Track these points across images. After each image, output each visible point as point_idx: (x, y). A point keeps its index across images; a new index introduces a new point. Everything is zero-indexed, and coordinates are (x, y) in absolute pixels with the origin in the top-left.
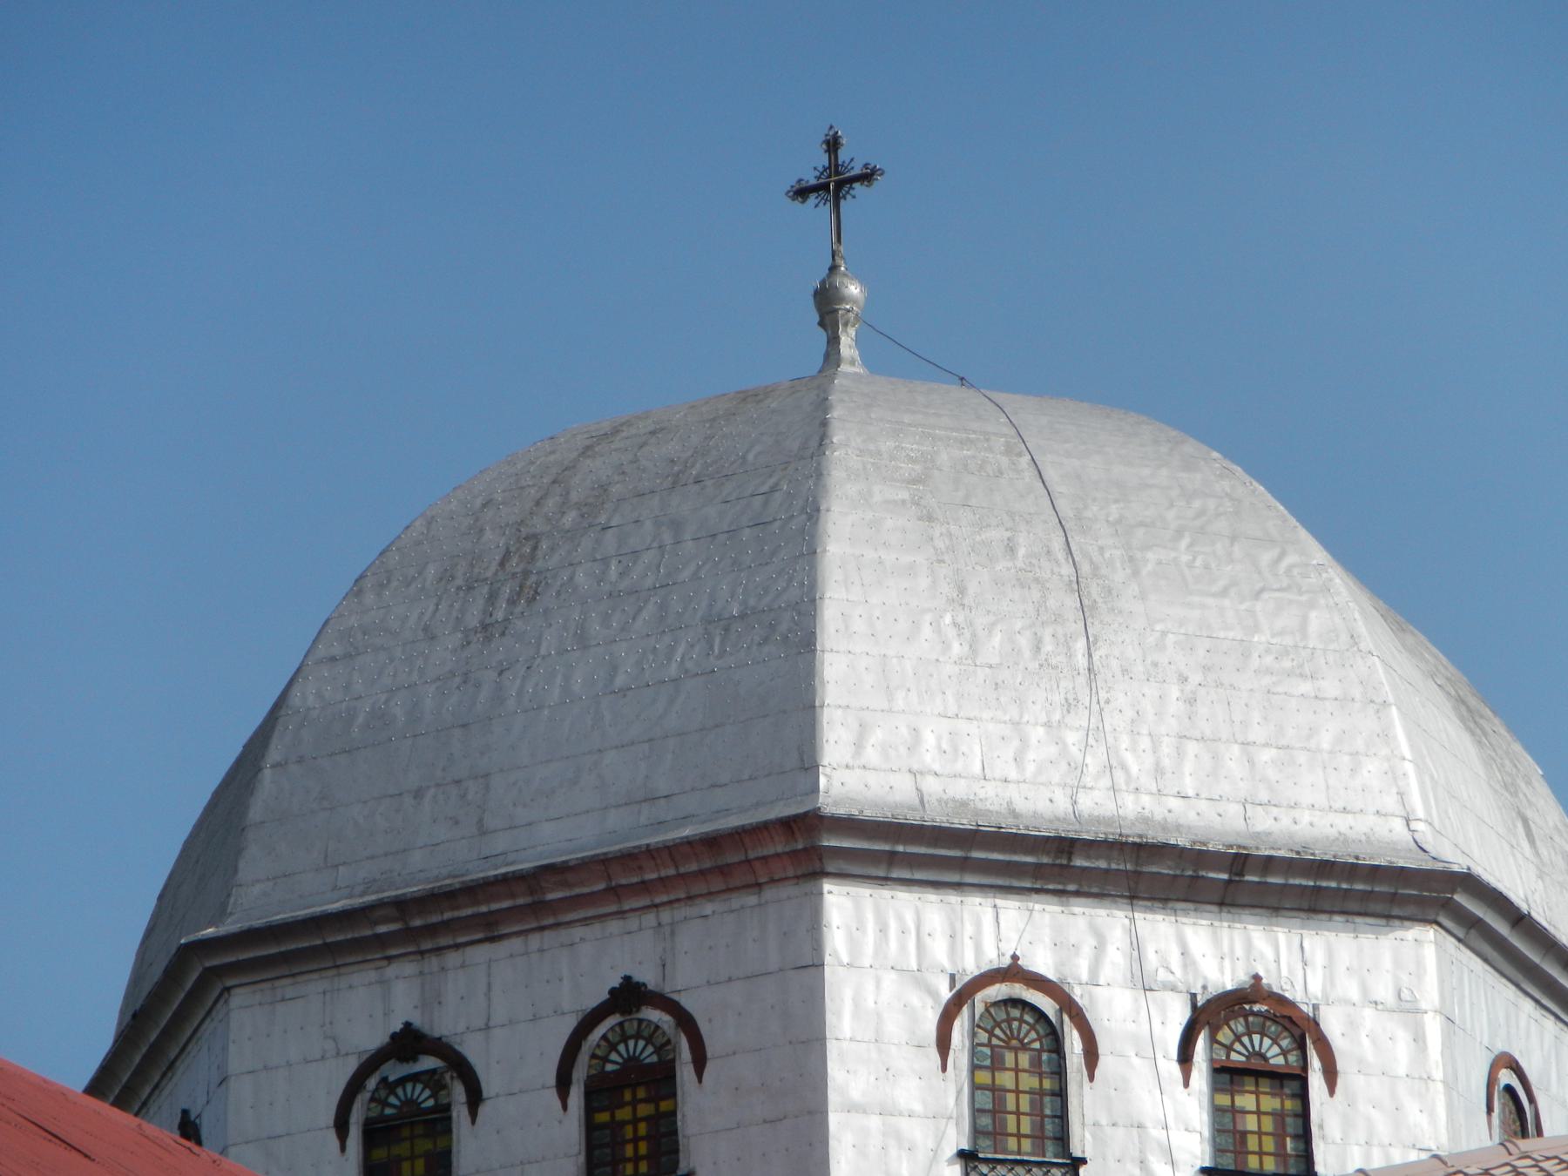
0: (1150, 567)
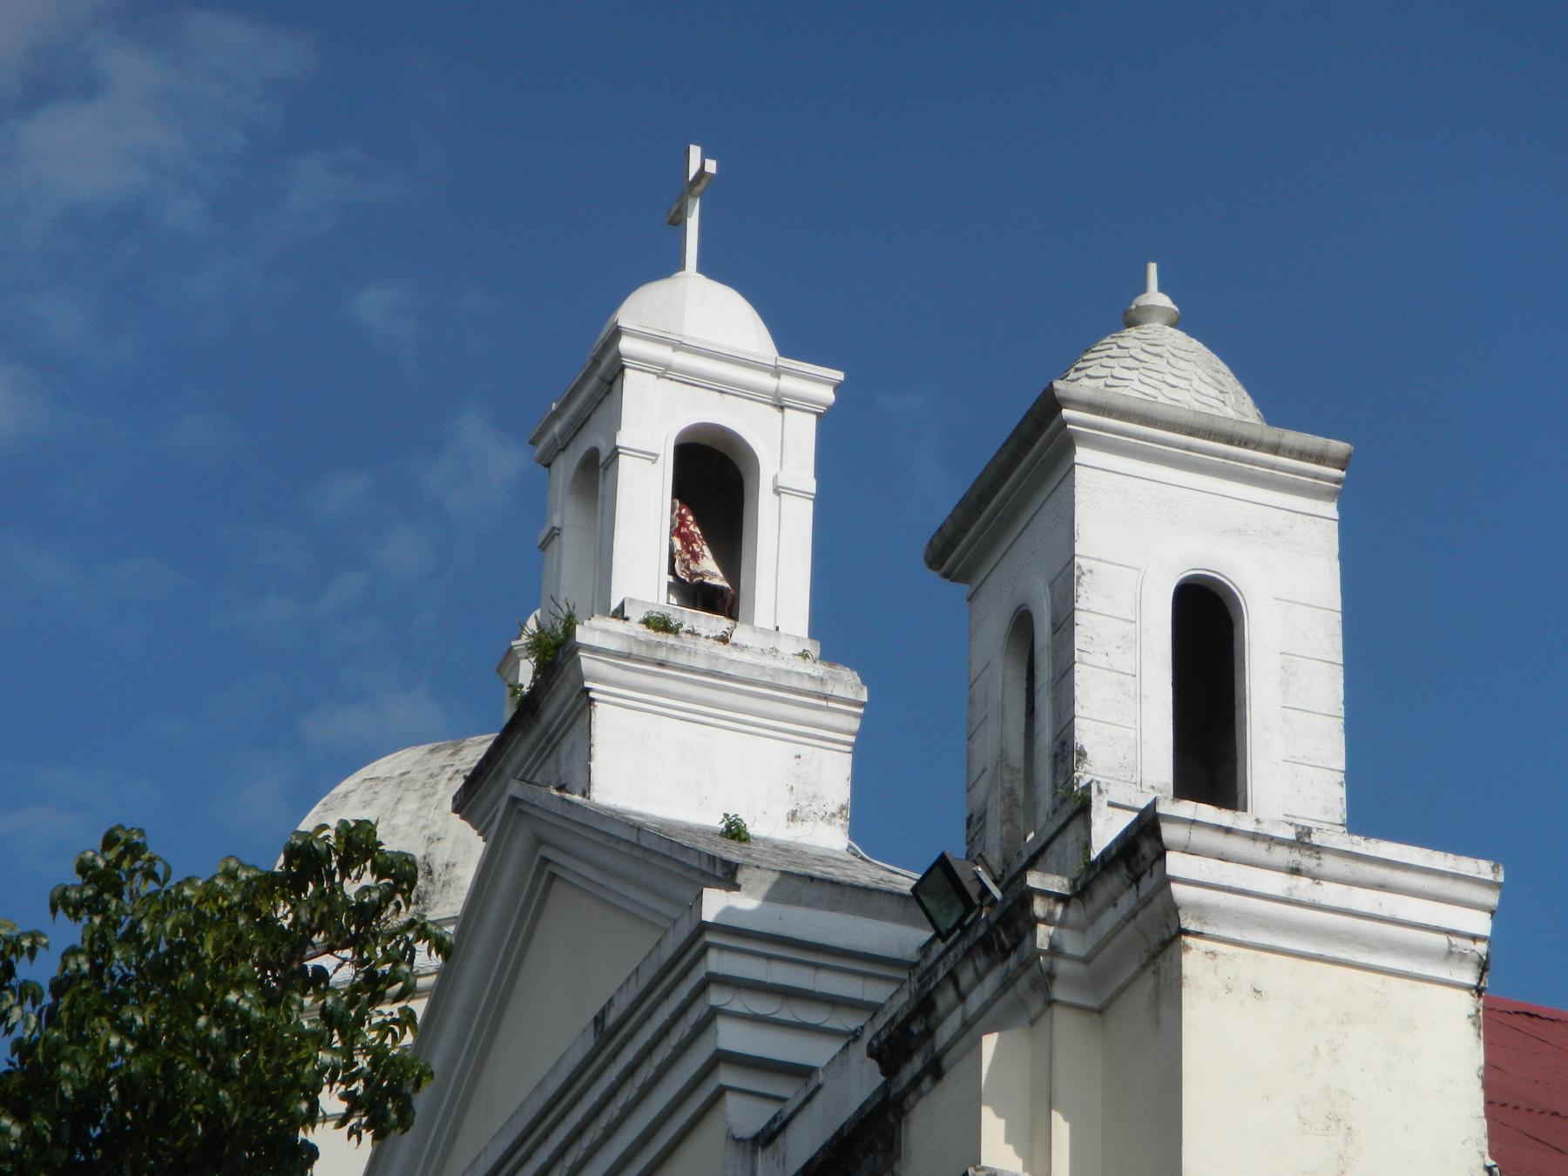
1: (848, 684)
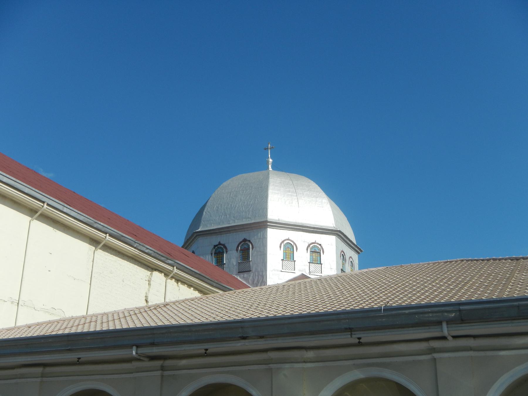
0: (305, 194)
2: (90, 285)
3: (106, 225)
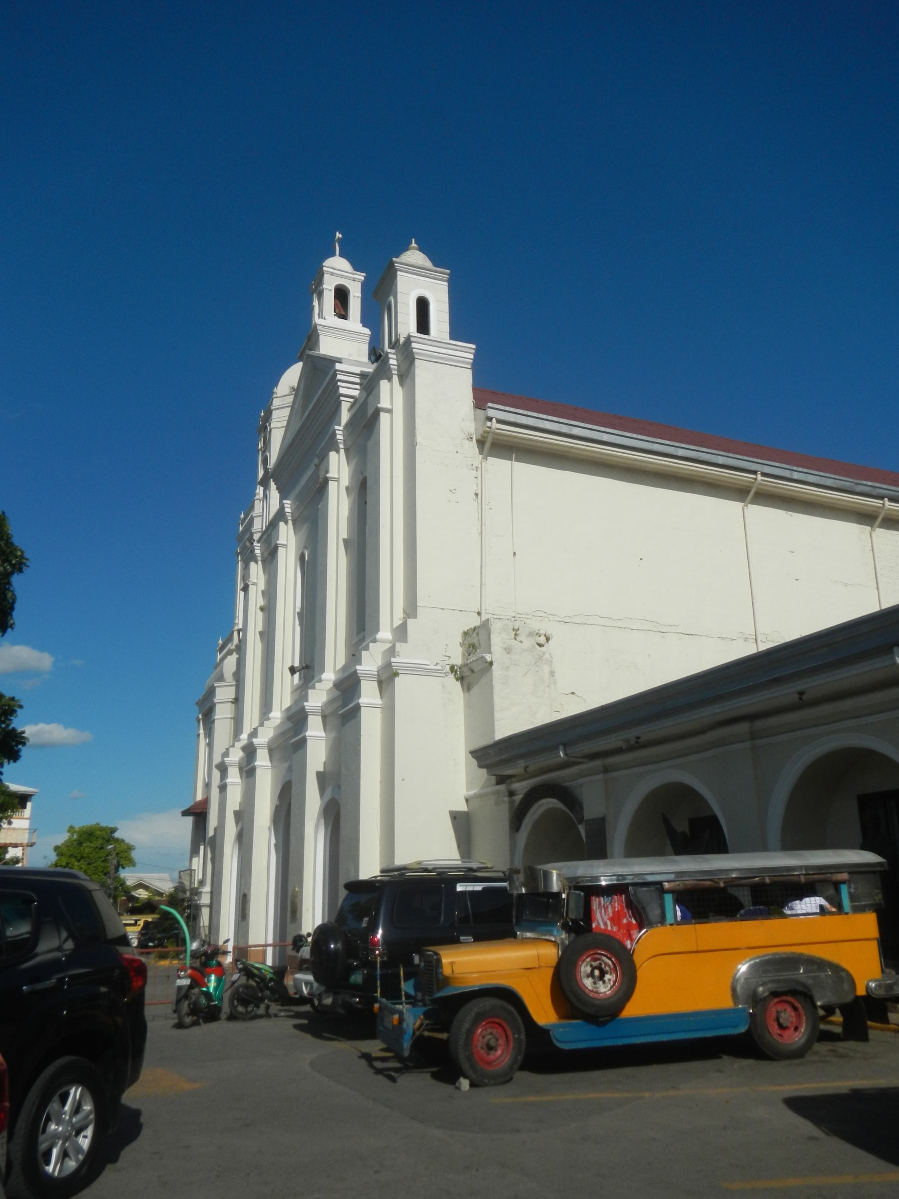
1: (367, 331)
2: (877, 589)
3: (877, 485)
